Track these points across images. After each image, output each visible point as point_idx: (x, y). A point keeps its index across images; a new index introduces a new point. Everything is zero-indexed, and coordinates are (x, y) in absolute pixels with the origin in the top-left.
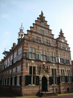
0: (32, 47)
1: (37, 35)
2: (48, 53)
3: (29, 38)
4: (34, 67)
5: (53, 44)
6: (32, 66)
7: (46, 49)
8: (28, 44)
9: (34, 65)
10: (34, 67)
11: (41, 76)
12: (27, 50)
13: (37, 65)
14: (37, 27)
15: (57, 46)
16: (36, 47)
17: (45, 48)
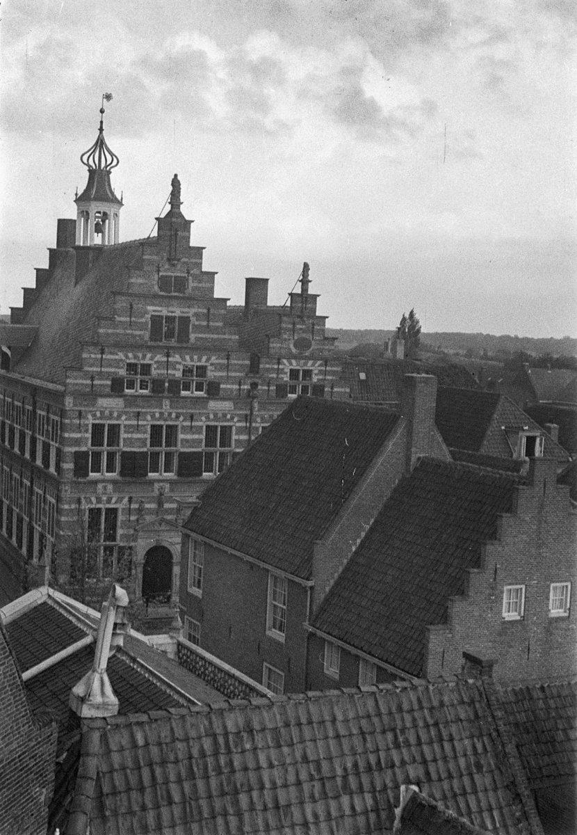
0: (104, 425)
1: (130, 355)
2: (189, 437)
3: (89, 382)
4: (112, 513)
5: (228, 379)
6: (99, 510)
7: (177, 417)
8: (83, 413)
9: (109, 501)
10: (112, 513)
11: (142, 546)
12: (77, 442)
13: (126, 500)
14: (135, 306)
15: (254, 385)
16: (124, 418)
17: (174, 415)
